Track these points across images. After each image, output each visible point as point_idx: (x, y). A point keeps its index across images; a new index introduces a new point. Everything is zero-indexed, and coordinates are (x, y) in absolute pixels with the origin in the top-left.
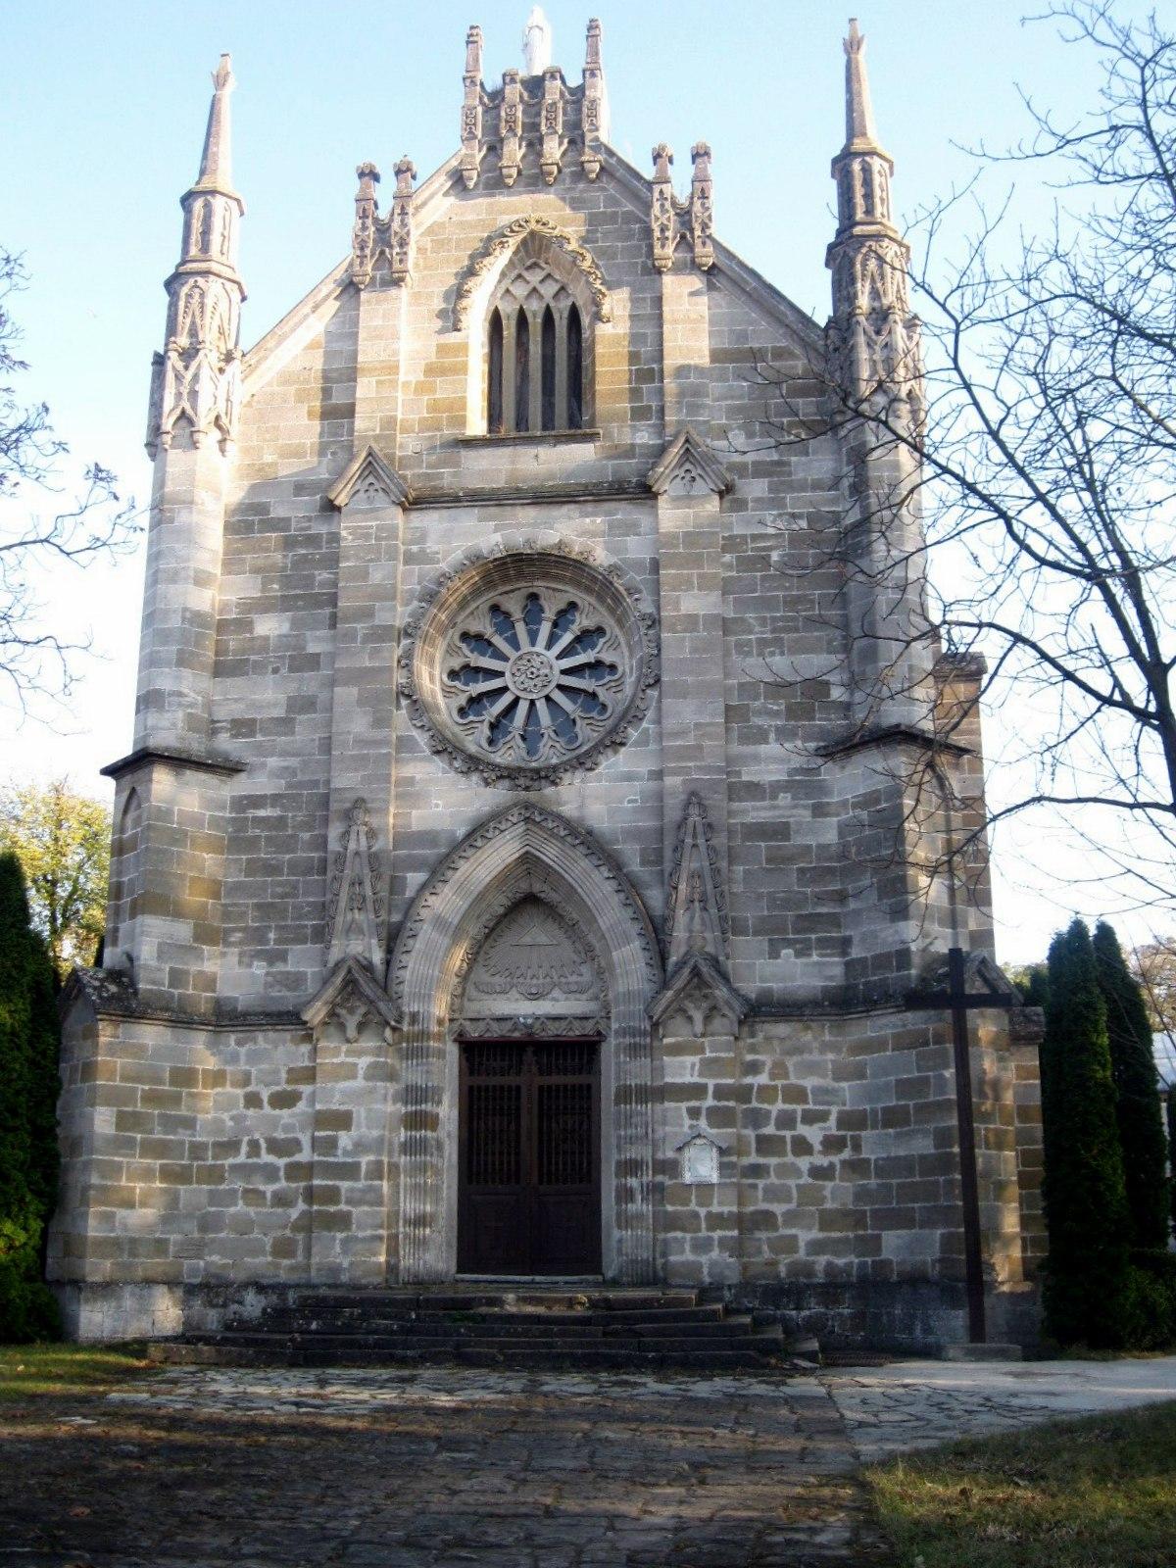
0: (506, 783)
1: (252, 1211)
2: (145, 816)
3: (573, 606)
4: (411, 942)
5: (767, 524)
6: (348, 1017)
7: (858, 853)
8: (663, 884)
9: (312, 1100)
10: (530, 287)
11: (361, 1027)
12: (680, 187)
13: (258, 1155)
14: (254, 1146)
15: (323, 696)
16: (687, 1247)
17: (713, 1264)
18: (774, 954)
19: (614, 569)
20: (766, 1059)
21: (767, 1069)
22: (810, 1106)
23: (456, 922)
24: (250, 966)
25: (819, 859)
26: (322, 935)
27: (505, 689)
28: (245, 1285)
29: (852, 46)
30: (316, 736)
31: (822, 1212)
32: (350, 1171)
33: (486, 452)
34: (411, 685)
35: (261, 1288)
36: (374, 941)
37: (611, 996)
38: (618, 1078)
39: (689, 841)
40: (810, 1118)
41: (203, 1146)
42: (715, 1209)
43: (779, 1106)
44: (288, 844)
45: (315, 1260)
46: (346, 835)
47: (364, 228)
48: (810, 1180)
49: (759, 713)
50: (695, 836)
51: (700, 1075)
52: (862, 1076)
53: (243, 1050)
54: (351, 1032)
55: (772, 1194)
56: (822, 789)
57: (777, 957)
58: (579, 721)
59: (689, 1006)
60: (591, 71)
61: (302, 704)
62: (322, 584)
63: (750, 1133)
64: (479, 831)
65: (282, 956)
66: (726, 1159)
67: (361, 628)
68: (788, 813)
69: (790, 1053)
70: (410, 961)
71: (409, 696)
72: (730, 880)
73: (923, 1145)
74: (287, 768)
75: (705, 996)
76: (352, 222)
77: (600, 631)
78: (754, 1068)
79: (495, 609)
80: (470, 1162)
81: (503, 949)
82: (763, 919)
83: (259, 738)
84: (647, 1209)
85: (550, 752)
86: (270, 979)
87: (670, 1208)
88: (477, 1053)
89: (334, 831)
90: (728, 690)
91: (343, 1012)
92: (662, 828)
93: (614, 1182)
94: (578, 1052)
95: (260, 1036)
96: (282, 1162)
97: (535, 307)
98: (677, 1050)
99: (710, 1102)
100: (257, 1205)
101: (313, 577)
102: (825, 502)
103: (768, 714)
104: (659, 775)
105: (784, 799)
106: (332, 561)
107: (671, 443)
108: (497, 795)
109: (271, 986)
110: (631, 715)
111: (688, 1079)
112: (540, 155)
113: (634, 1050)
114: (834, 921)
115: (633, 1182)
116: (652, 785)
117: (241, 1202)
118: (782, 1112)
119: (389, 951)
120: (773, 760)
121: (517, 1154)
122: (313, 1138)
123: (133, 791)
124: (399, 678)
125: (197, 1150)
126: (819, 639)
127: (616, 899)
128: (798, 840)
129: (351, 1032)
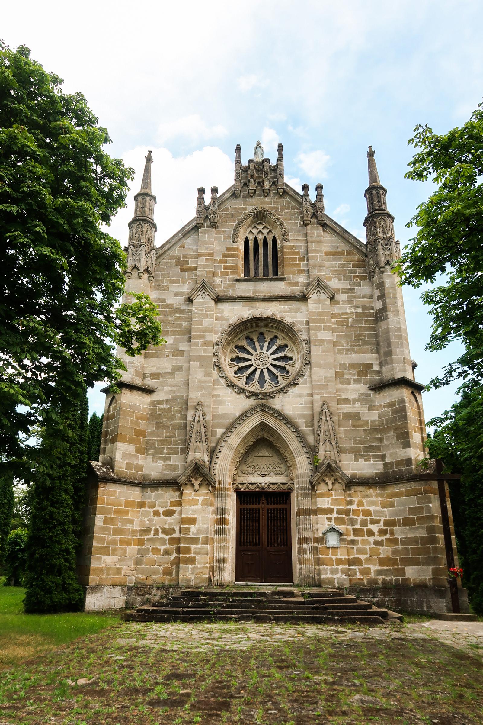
0: (254, 397)
1: (155, 557)
2: (118, 406)
4: (219, 454)
5: (347, 309)
6: (195, 481)
7: (387, 423)
8: (314, 434)
9: (180, 513)
10: (259, 230)
11: (200, 485)
13: (158, 535)
14: (157, 532)
15: (185, 365)
16: (329, 572)
17: (339, 579)
18: (356, 460)
19: (293, 324)
20: (356, 499)
21: (356, 503)
22: (373, 518)
23: (236, 447)
24: (157, 462)
25: (372, 426)
26: (185, 451)
27: (252, 365)
28: (152, 587)
29: (371, 154)
30: (183, 379)
31: (380, 559)
32: (195, 541)
33: (245, 283)
34: (219, 362)
35: (158, 588)
36: (205, 454)
37: (294, 475)
38: (298, 505)
39: (324, 418)
40: (373, 522)
42: (339, 557)
43: (361, 517)
44: (172, 418)
45: (181, 576)
46: (195, 414)
48: (374, 546)
50: (326, 417)
51: (331, 505)
52: (394, 506)
53: (153, 494)
54: (196, 487)
55: (361, 551)
56: (371, 401)
57: (358, 461)
58: (279, 377)
60: (280, 159)
61: (177, 368)
62: (185, 327)
63: (350, 528)
64: (244, 416)
65: (169, 459)
66: (342, 537)
67: (200, 342)
68: (359, 409)
71: (218, 366)
72: (340, 433)
74: (171, 391)
75: (332, 476)
78: (350, 503)
80: (241, 538)
81: (252, 460)
82: (352, 448)
86: (164, 467)
87: (321, 556)
90: (335, 366)
91: (193, 480)
92: (313, 415)
94: (282, 497)
95: (160, 490)
96: (167, 537)
97: (260, 237)
98: (322, 495)
99: (335, 515)
100: (157, 554)
101: (181, 325)
102: (366, 303)
103: (350, 375)
104: (311, 395)
105: (358, 404)
106: (190, 319)
108: (252, 402)
109: (165, 470)
110: (300, 374)
112: (262, 186)
113: (305, 496)
114: (378, 448)
115: (306, 546)
116: (309, 399)
117: (151, 553)
118: (362, 520)
119: (211, 457)
121: (259, 534)
122: (180, 528)
123: (114, 398)
124: (215, 360)
125: (134, 532)
126: (368, 349)
128: (363, 419)
129: (196, 487)
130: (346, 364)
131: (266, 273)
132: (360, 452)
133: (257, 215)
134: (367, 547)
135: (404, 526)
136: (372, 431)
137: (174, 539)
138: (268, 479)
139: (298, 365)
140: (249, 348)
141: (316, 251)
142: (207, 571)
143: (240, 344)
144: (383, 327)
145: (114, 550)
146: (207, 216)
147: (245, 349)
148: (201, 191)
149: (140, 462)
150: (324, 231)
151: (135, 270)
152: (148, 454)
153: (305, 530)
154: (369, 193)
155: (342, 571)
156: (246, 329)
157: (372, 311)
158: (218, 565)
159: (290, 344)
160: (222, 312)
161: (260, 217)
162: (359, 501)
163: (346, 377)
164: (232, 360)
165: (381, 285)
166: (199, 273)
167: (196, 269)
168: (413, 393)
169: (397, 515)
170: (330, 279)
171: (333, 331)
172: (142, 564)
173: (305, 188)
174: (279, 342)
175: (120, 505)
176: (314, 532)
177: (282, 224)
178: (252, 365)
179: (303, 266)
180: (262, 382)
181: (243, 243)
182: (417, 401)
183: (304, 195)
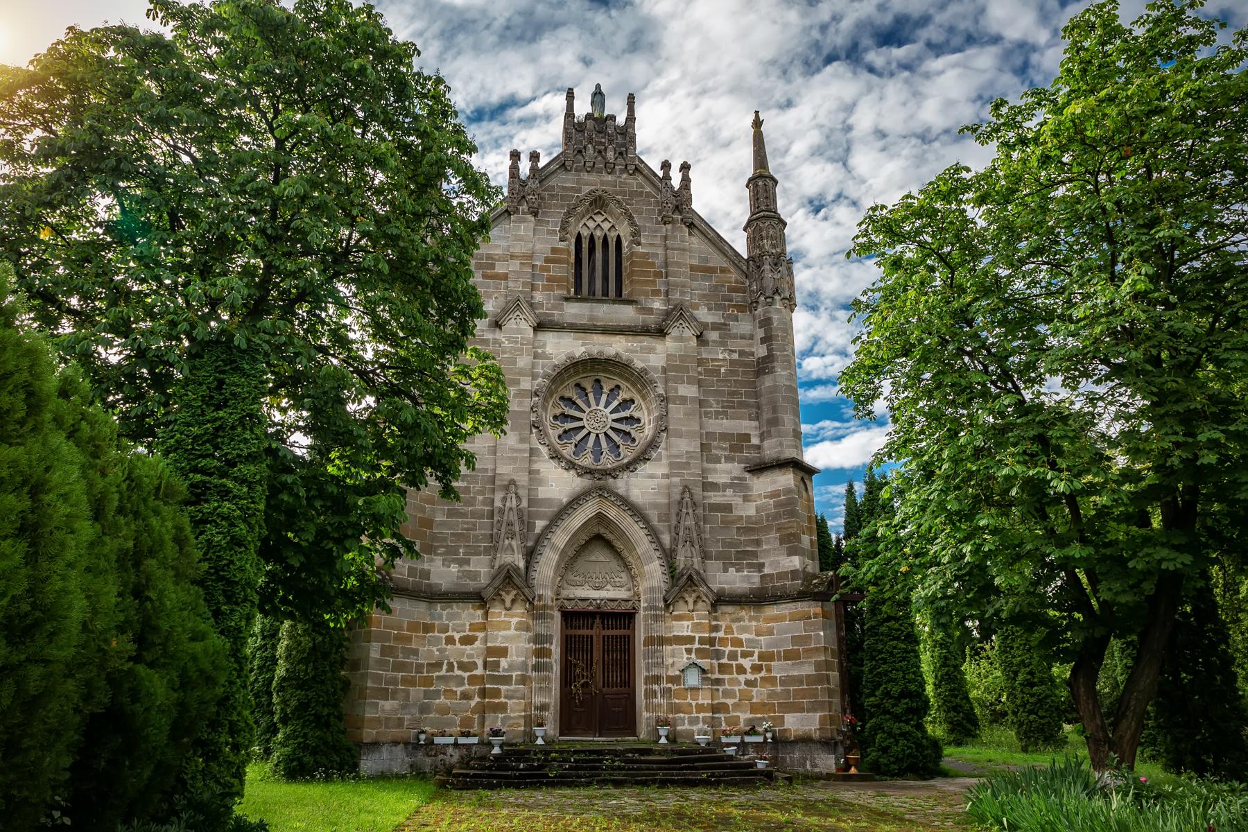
0: (589, 476)
1: (448, 702)
3: (618, 387)
9: (486, 640)
11: (513, 601)
12: (676, 181)
18: (726, 571)
20: (723, 624)
27: (583, 427)
32: (506, 680)
38: (646, 630)
40: (745, 655)
41: (422, 665)
42: (700, 702)
46: (504, 499)
49: (716, 448)
54: (508, 604)
55: (727, 694)
59: (686, 596)
60: (631, 118)
63: (715, 662)
64: (576, 501)
65: (468, 562)
69: (733, 621)
70: (537, 567)
73: (808, 670)
77: (632, 401)
78: (716, 629)
79: (578, 385)
81: (581, 565)
84: (663, 702)
85: (608, 461)
88: (570, 617)
89: (498, 497)
95: (454, 606)
96: (466, 675)
98: (680, 618)
99: (697, 645)
104: (667, 476)
105: (729, 492)
110: (652, 445)
113: (656, 618)
114: (754, 554)
115: (656, 687)
120: (724, 471)
125: (419, 668)
127: (646, 540)
128: (736, 513)
129: (508, 604)
130: (714, 433)
131: (605, 292)
132: (730, 558)
133: (595, 200)
134: (736, 688)
138: (603, 594)
139: (649, 431)
140: (579, 402)
141: (679, 264)
142: (522, 722)
143: (567, 394)
144: (767, 384)
145: (395, 692)
146: (524, 197)
147: (574, 403)
148: (515, 156)
149: (426, 566)
150: (690, 234)
153: (656, 665)
156: (577, 373)
157: (751, 358)
158: (537, 713)
159: (637, 398)
160: (544, 346)
161: (598, 203)
162: (727, 627)
163: (714, 452)
164: (555, 417)
165: (766, 323)
168: (802, 479)
169: (776, 646)
170: (696, 307)
171: (700, 384)
172: (430, 712)
173: (666, 166)
174: (623, 395)
175: (401, 628)
177: (631, 218)
178: (583, 427)
179: (660, 285)
180: (598, 453)
181: (573, 240)
182: (807, 490)
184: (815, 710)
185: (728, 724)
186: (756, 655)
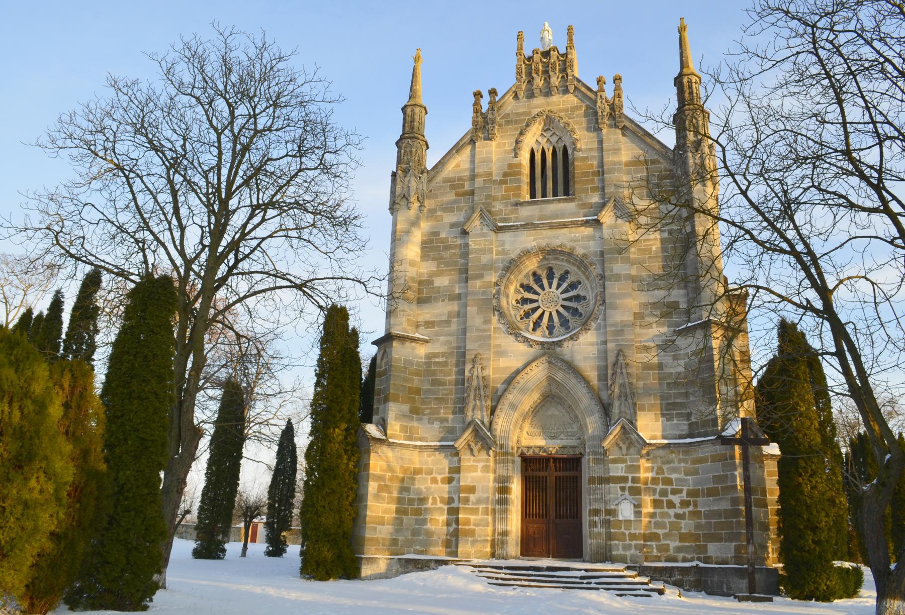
3: (567, 272)
11: (479, 450)
12: (609, 93)
17: (632, 556)
19: (585, 255)
29: (681, 30)
39: (619, 371)
40: (675, 492)
41: (413, 500)
42: (633, 531)
43: (661, 486)
47: (477, 117)
52: (697, 474)
60: (570, 46)
62: (462, 265)
69: (664, 463)
73: (725, 505)
75: (628, 439)
76: (471, 114)
83: (436, 328)
84: (603, 531)
87: (612, 530)
89: (468, 367)
93: (588, 518)
98: (615, 461)
99: (630, 484)
107: (608, 202)
111: (620, 474)
112: (549, 83)
114: (683, 405)
115: (596, 519)
116: (602, 347)
118: (662, 490)
134: (667, 520)
135: (708, 496)
136: (676, 384)
137: (453, 508)
140: (536, 287)
148: (478, 95)
151: (404, 200)
152: (424, 415)
154: (678, 81)
155: (637, 547)
159: (583, 278)
166: (476, 198)
167: (472, 193)
173: (599, 81)
174: (571, 278)
176: (606, 503)
183: (599, 91)
184: (731, 541)
185: (659, 550)
186: (685, 492)
